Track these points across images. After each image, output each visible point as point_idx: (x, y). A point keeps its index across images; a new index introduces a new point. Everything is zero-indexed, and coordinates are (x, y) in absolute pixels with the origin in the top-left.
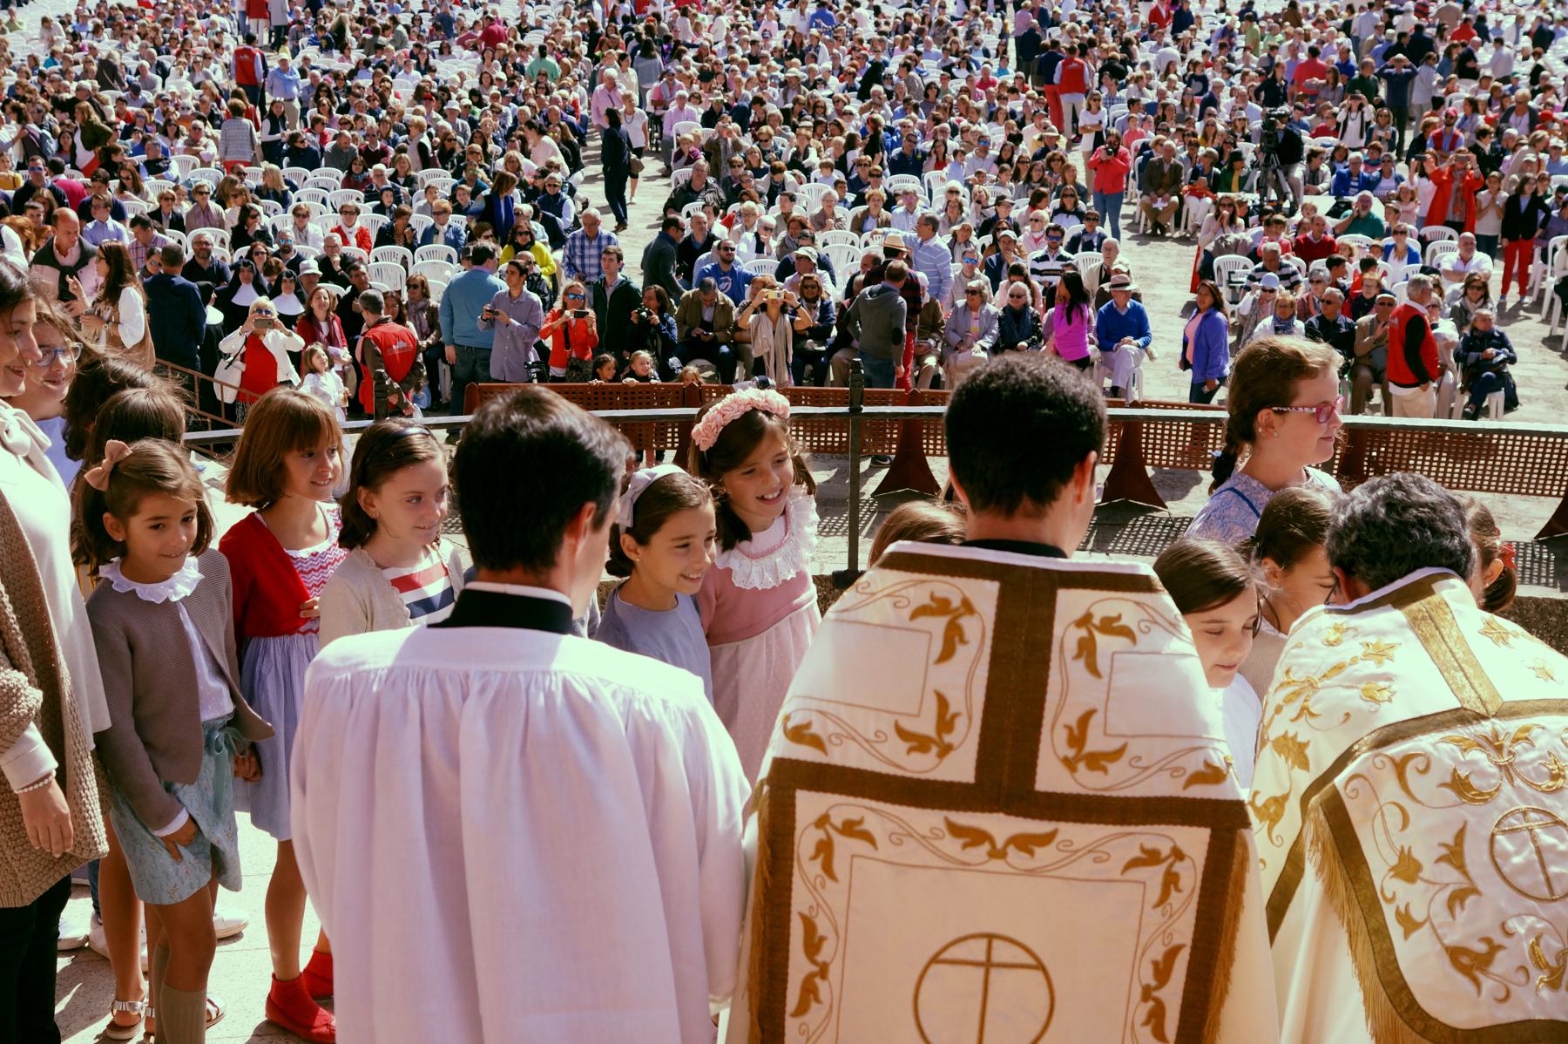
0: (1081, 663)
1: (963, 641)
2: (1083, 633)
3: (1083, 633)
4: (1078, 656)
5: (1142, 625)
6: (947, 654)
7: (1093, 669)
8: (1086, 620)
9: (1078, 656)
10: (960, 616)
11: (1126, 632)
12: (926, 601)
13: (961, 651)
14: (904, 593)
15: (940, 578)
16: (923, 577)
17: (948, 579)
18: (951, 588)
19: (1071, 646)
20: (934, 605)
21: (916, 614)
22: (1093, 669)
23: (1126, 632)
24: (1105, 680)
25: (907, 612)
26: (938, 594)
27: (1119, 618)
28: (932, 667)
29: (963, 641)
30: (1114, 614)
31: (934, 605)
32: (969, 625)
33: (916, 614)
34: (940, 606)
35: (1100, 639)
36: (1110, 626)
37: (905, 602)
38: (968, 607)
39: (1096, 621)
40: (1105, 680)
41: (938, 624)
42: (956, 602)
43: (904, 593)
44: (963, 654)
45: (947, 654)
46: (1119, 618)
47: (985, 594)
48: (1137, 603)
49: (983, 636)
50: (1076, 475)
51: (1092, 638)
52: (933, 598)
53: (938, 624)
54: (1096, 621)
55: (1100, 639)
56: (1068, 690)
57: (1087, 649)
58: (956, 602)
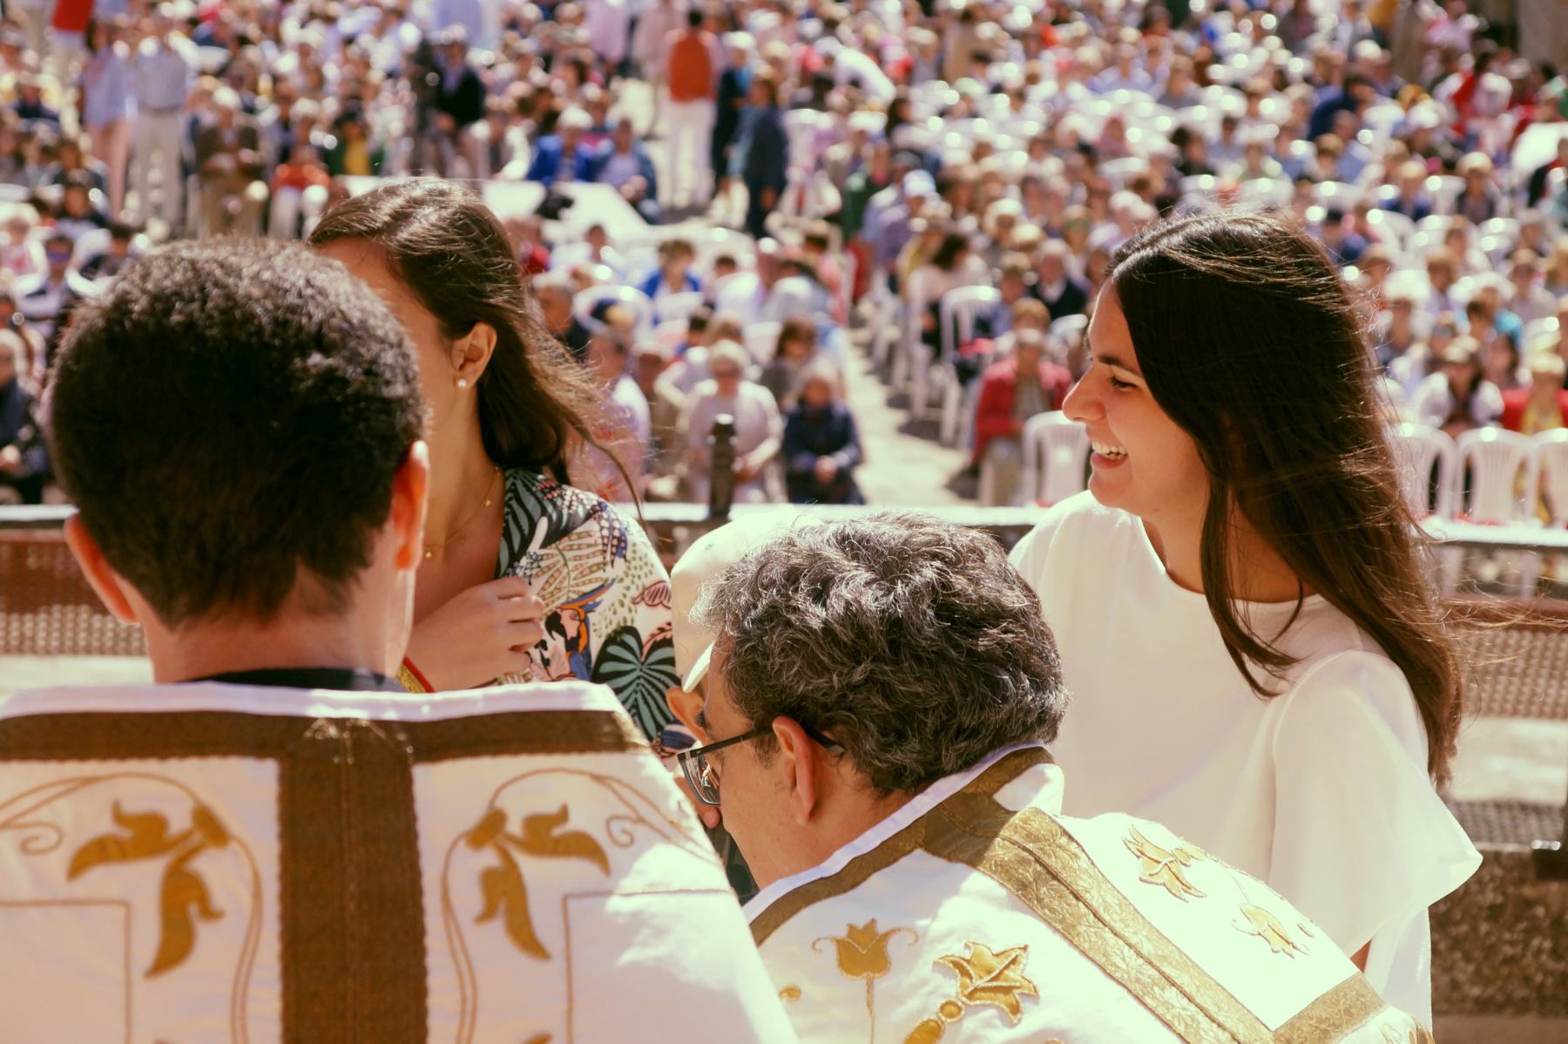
0: (497, 928)
1: (210, 914)
2: (489, 858)
3: (489, 858)
4: (487, 915)
5: (616, 827)
6: (175, 948)
7: (529, 943)
8: (490, 828)
9: (487, 915)
10: (195, 851)
11: (584, 847)
12: (104, 826)
13: (207, 935)
14: (44, 814)
15: (132, 765)
16: (91, 768)
17: (152, 766)
18: (166, 787)
19: (468, 899)
20: (126, 834)
21: (80, 863)
22: (529, 943)
23: (584, 847)
24: (556, 966)
25: (57, 863)
26: (132, 806)
27: (563, 816)
28: (145, 990)
29: (210, 914)
30: (550, 807)
31: (126, 834)
32: (211, 867)
33: (80, 863)
34: (141, 836)
35: (531, 868)
36: (548, 835)
37: (52, 837)
38: (211, 829)
39: (514, 827)
40: (556, 966)
41: (142, 880)
42: (179, 821)
43: (44, 814)
44: (215, 944)
45: (175, 948)
46: (563, 816)
47: (247, 790)
48: (598, 778)
49: (257, 895)
50: (397, 502)
51: (511, 868)
52: (119, 817)
53: (142, 880)
54: (514, 827)
55: (531, 868)
56: (477, 1003)
57: (504, 895)
58: (179, 821)
